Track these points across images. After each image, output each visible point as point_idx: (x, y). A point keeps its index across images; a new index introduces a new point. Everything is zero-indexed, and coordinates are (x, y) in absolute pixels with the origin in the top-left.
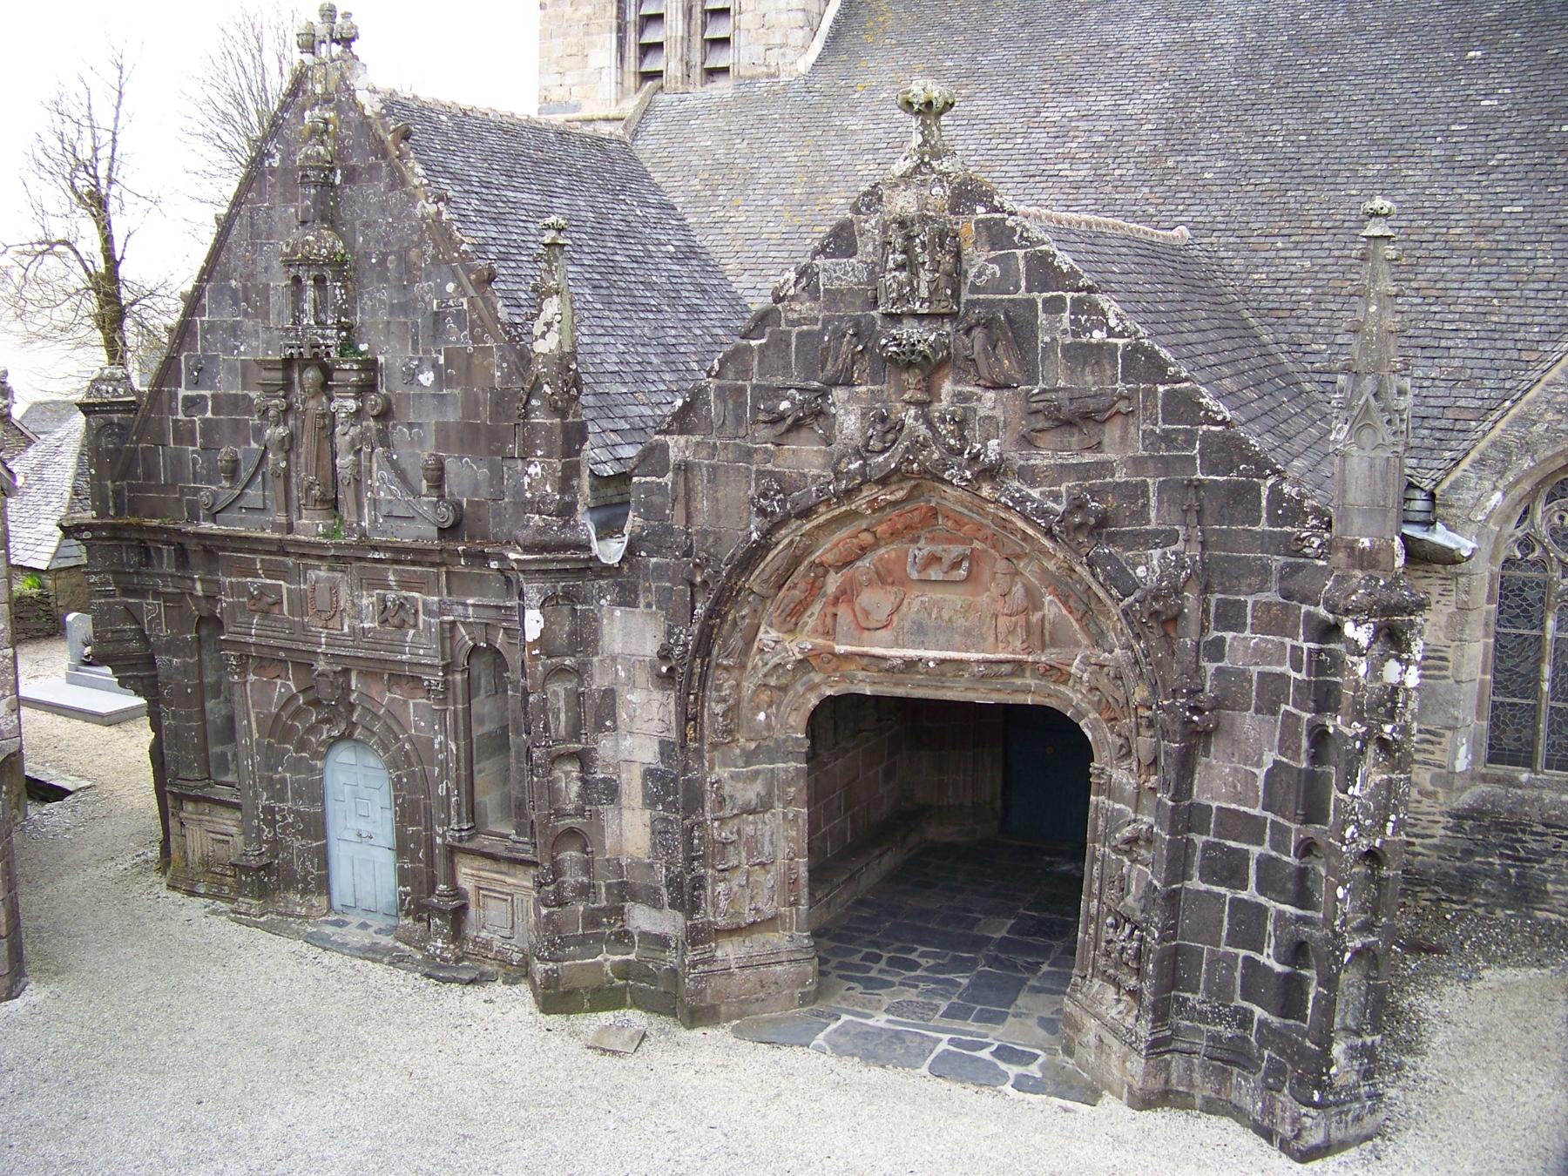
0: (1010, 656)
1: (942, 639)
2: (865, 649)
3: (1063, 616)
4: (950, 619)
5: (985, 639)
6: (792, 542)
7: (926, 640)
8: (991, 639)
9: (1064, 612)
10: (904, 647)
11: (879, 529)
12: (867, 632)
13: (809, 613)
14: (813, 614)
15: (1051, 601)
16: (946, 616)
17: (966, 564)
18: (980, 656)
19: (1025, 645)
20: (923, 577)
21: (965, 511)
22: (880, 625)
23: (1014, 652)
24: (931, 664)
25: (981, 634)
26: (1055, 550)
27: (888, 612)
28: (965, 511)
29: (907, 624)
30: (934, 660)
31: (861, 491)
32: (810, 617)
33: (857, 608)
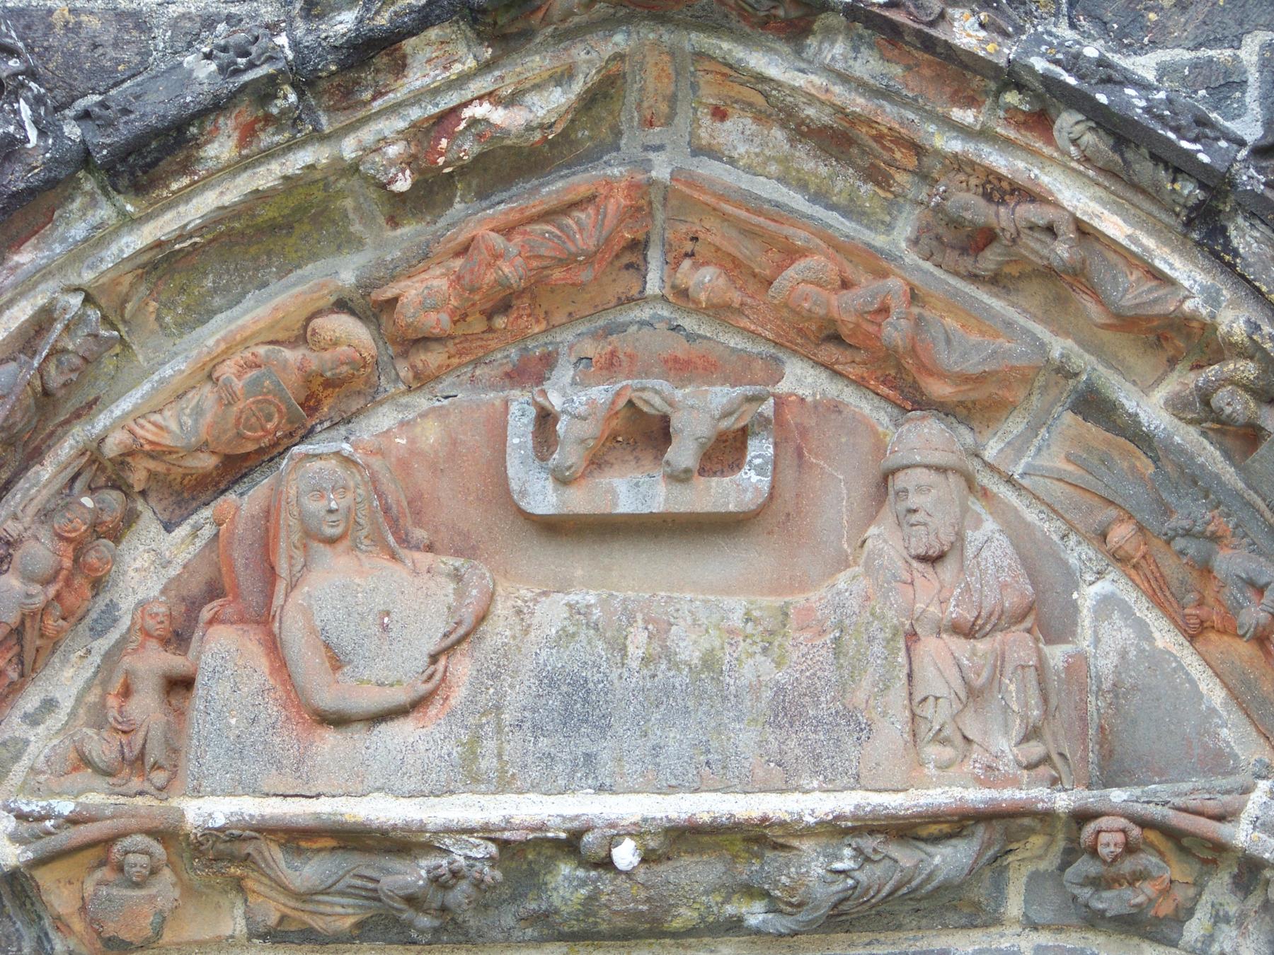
0: (976, 796)
1: (675, 741)
2: (326, 808)
3: (1156, 659)
4: (710, 662)
5: (864, 731)
6: (42, 321)
7: (605, 751)
8: (892, 730)
9: (1165, 637)
10: (504, 784)
11: (411, 291)
12: (330, 739)
13: (30, 701)
14: (49, 705)
15: (1107, 604)
16: (689, 648)
17: (760, 449)
18: (846, 802)
19: (1035, 750)
20: (579, 501)
21: (798, 201)
22: (400, 696)
23: (989, 776)
24: (626, 855)
25: (849, 715)
26: (1212, 298)
27: (431, 646)
28: (798, 201)
29: (517, 695)
30: (637, 832)
31: (400, 67)
32: (33, 720)
33: (293, 628)
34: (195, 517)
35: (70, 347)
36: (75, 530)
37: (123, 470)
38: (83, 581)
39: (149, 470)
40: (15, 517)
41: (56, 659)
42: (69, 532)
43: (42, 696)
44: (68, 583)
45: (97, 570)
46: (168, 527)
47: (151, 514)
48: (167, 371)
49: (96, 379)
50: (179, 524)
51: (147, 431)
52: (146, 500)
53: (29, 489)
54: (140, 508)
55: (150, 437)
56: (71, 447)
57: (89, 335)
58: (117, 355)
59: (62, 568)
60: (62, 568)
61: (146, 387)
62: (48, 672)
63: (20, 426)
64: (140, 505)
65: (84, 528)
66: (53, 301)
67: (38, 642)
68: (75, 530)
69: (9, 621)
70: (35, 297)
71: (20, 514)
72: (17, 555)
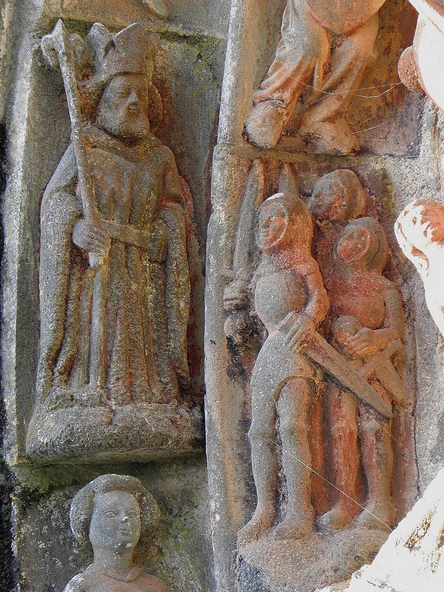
34: (425, 117)
35: (103, 77)
36: (280, 230)
37: (315, 147)
38: (357, 274)
39: (330, 120)
40: (226, 281)
41: (422, 375)
42: (275, 238)
43: (436, 420)
44: (333, 288)
45: (356, 250)
46: (413, 154)
47: (390, 161)
48: (233, 11)
49: (202, 95)
50: (418, 141)
51: (273, 82)
52: (373, 154)
53: (216, 243)
54: (378, 167)
55: (277, 84)
56: (221, 169)
57: (107, 50)
58: (200, 56)
59: (303, 278)
60: (303, 278)
61: (230, 45)
62: (422, 394)
63: (126, 191)
64: (374, 165)
65: (286, 220)
66: (38, 52)
67: (364, 372)
68: (280, 230)
69: (292, 373)
70: (22, 68)
71: (228, 273)
72: (260, 309)
